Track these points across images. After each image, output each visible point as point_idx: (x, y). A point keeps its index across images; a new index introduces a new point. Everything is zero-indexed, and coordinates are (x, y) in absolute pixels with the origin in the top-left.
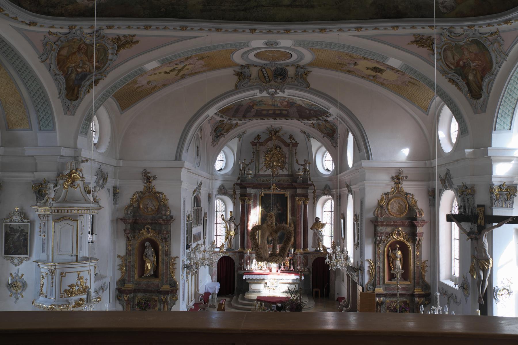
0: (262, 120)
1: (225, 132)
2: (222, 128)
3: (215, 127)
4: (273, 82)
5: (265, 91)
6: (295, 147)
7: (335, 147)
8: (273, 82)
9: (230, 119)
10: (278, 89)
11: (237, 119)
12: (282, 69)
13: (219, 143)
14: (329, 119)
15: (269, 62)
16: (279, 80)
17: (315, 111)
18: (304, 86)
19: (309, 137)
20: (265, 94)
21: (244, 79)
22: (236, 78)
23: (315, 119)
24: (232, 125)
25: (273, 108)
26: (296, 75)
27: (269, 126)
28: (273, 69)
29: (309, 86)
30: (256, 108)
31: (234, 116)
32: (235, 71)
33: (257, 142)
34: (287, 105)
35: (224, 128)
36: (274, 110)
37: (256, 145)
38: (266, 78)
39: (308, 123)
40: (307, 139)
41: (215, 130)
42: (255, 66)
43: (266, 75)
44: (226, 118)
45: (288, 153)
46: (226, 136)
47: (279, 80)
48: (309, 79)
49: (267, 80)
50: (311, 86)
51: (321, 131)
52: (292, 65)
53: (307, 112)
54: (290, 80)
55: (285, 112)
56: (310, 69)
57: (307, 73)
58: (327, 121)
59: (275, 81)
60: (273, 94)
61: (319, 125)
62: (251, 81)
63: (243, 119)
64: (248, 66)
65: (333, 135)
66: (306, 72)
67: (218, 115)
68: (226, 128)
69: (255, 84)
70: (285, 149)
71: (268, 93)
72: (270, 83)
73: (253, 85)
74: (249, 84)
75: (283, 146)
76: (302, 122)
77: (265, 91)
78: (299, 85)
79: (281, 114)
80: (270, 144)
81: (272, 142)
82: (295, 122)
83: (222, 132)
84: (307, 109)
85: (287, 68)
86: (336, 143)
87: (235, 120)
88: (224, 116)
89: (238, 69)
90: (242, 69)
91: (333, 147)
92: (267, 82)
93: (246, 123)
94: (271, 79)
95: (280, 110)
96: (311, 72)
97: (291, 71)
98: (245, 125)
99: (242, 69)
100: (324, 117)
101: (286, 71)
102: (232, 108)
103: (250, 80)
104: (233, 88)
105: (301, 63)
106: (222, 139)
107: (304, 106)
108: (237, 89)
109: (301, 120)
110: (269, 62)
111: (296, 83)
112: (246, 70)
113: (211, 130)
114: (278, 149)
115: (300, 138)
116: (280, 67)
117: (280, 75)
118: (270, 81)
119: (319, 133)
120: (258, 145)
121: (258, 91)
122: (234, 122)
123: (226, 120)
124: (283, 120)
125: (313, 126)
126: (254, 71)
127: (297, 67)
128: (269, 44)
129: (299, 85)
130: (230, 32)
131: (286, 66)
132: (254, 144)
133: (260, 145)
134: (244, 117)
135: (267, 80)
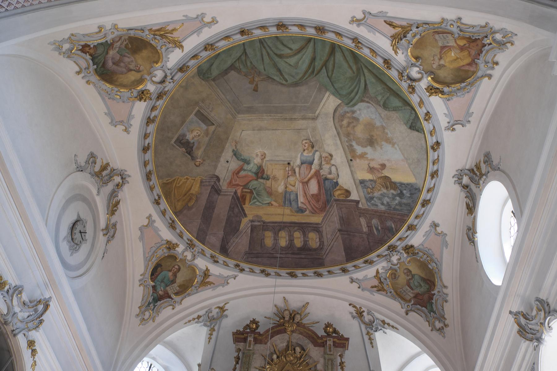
1: (177, 294)
3: (155, 261)
6: (340, 349)
7: (440, 330)
13: (159, 319)
17: (380, 216)
19: (371, 326)
23: (383, 250)
24: (193, 269)
25: (286, 215)
33: (248, 335)
34: (316, 197)
35: (175, 275)
37: (245, 340)
39: (366, 278)
40: (366, 338)
41: (154, 274)
45: (322, 361)
46: (178, 308)
51: (399, 295)
55: (313, 240)
58: (412, 246)
63: (221, 258)
65: (431, 297)
68: (180, 279)
70: (315, 352)
75: (310, 347)
76: (352, 281)
79: (305, 248)
80: (280, 342)
81: (286, 336)
83: (170, 290)
84: (363, 213)
86: (442, 318)
87: (203, 253)
88: (180, 226)
91: (435, 334)
95: (303, 227)
98: (227, 289)
106: (167, 312)
107: (354, 196)
109: (349, 266)
113: (142, 270)
114: (298, 349)
115: (351, 329)
119: (396, 305)
120: (250, 339)
122: (201, 263)
123: (181, 248)
125: (380, 287)
132: (240, 336)
133: (256, 341)
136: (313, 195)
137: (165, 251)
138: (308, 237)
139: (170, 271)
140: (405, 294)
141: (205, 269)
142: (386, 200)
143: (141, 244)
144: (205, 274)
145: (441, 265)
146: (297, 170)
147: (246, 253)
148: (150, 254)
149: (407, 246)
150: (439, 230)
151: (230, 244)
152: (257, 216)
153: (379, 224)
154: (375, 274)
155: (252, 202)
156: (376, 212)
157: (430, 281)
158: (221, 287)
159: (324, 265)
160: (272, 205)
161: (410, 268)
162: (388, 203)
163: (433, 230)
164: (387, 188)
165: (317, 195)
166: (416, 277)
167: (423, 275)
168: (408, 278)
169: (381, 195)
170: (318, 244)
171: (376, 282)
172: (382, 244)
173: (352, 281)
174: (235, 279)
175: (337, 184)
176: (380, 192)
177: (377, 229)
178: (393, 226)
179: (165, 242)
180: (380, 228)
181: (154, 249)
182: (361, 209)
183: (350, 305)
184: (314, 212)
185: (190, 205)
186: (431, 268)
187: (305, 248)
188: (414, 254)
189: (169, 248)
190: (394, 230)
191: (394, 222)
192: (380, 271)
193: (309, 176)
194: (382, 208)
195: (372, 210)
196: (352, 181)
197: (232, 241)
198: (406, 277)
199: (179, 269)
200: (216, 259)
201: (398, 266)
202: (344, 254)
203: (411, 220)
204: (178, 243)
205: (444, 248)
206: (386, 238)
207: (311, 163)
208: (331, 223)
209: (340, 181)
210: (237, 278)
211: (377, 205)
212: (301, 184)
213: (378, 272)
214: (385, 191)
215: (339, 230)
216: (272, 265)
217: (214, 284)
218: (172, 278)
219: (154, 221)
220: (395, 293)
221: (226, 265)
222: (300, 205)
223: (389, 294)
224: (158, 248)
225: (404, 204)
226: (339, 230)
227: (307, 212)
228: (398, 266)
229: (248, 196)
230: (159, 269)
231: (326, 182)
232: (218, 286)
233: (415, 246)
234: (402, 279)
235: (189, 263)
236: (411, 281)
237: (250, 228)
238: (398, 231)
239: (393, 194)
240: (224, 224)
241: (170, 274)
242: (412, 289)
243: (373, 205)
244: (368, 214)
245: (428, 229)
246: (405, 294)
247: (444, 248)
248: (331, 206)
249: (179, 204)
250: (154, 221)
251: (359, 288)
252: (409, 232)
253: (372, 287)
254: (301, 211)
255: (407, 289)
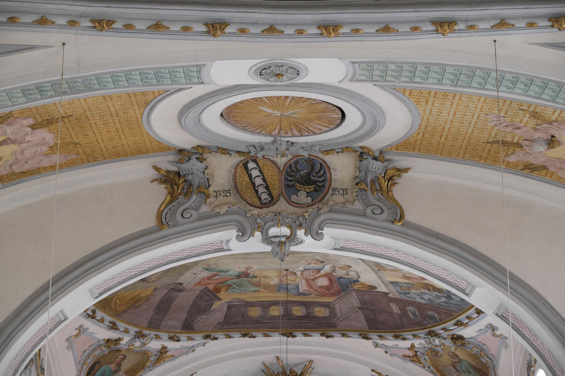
0: (247, 339)
2: (113, 366)
3: (90, 362)
4: (282, 205)
5: (258, 234)
8: (282, 205)
9: (140, 335)
10: (300, 226)
11: (165, 336)
12: (311, 162)
14: (467, 333)
15: (269, 139)
16: (302, 197)
17: (418, 306)
18: (385, 215)
20: (255, 244)
21: (188, 194)
22: (160, 192)
23: (422, 333)
24: (145, 355)
25: (281, 296)
26: (358, 182)
27: (269, 358)
28: (282, 161)
29: (402, 217)
30: (226, 297)
31: (155, 325)
32: (157, 169)
34: (328, 288)
35: (119, 365)
36: (286, 304)
38: (261, 190)
39: (396, 347)
42: (224, 151)
43: (258, 181)
44: (126, 331)
47: (302, 197)
48: (399, 193)
49: (264, 196)
50: (409, 217)
52: (345, 149)
53: (395, 308)
54: (338, 198)
55: (320, 312)
56: (402, 161)
57: (393, 176)
58: (461, 338)
59: (290, 202)
60: (281, 244)
61: (434, 353)
62: (211, 200)
63: (183, 337)
64: (200, 153)
66: (390, 173)
67: (102, 321)
69: (225, 209)
71: (267, 240)
72: (274, 208)
73: (218, 214)
74: (204, 209)
76: (377, 346)
77: (258, 234)
78: (369, 211)
79: (308, 317)
82: (355, 344)
84: (396, 301)
85: (327, 158)
87: (158, 337)
89: (166, 162)
90: (179, 162)
92: (264, 205)
93: (192, 349)
94: (275, 193)
95: (306, 305)
96: (406, 170)
97: (342, 169)
98: (191, 355)
99: (179, 162)
100: (449, 325)
101: (324, 167)
102: (148, 298)
103: (208, 196)
104: (150, 222)
105: (375, 143)
107: (382, 288)
108: (165, 224)
110: (269, 139)
111: (358, 206)
112: (194, 165)
116: (306, 154)
117: (307, 181)
118: (272, 201)
121: (232, 233)
122: (154, 345)
124: (316, 339)
126: (221, 170)
127: (362, 154)
128: (272, 72)
129: (369, 211)
130: (141, 32)
131: (327, 152)
134: (188, 327)
135: (264, 196)
136: (321, 287)
137: (103, 348)
138: (313, 310)
139: (112, 363)
140: (448, 373)
141: (161, 347)
142: (426, 297)
143: (70, 352)
144: (161, 353)
145: (498, 361)
146: (299, 274)
147: (219, 324)
148: (83, 357)
149: (454, 335)
150: (497, 333)
151: (196, 321)
152: (237, 299)
153: (416, 311)
154: (409, 346)
155: (230, 291)
156: (412, 302)
157: (482, 371)
158: (184, 356)
159: (336, 328)
160: (259, 291)
161: (457, 353)
162: (429, 299)
163: (490, 331)
164: (429, 290)
165: (326, 286)
166: (464, 362)
167: (474, 364)
168: (454, 360)
169: (421, 292)
170: (329, 314)
171: (411, 353)
172: (419, 326)
173: (377, 346)
174: (204, 346)
175: (357, 281)
176: (419, 291)
177: (414, 314)
178: (436, 316)
179: (104, 342)
180: (417, 314)
181: (88, 352)
182: (392, 298)
183: (373, 371)
184: (322, 295)
185: (137, 305)
186: (485, 362)
187: (308, 317)
188: (463, 345)
189: (109, 347)
190: (438, 319)
191: (438, 313)
192: (416, 346)
193: (317, 276)
194: (423, 301)
195: (408, 301)
196: (380, 281)
197: (199, 318)
198: (451, 359)
199: (125, 357)
200: (176, 338)
201: (442, 347)
202: (365, 323)
203: (462, 317)
204: (121, 337)
205: (503, 348)
206: (425, 322)
207: (319, 270)
208: (347, 304)
209: (362, 280)
210: (206, 345)
211: (415, 299)
212: (304, 281)
213: (413, 346)
214: (426, 291)
215: (359, 308)
216: (258, 329)
217: (174, 356)
218: (115, 368)
219: (87, 329)
220: (435, 371)
221: (190, 339)
222: (301, 291)
223: (426, 368)
224: (95, 349)
225: (453, 304)
226: (359, 308)
227: (313, 295)
228: (442, 347)
229: (224, 289)
230: (97, 366)
231: (341, 279)
232: (178, 357)
233: (465, 337)
234: (445, 359)
235: (138, 349)
236: (458, 365)
237: (226, 307)
238: (442, 321)
239: (437, 295)
240: (187, 309)
241: (113, 365)
242: (458, 372)
243: (408, 297)
244: (403, 304)
245: (484, 328)
246: (448, 373)
247: (503, 348)
248: (348, 293)
249: (122, 307)
250: (87, 329)
251: (386, 352)
252: (456, 327)
253: (405, 356)
254: (304, 294)
255: (451, 370)
